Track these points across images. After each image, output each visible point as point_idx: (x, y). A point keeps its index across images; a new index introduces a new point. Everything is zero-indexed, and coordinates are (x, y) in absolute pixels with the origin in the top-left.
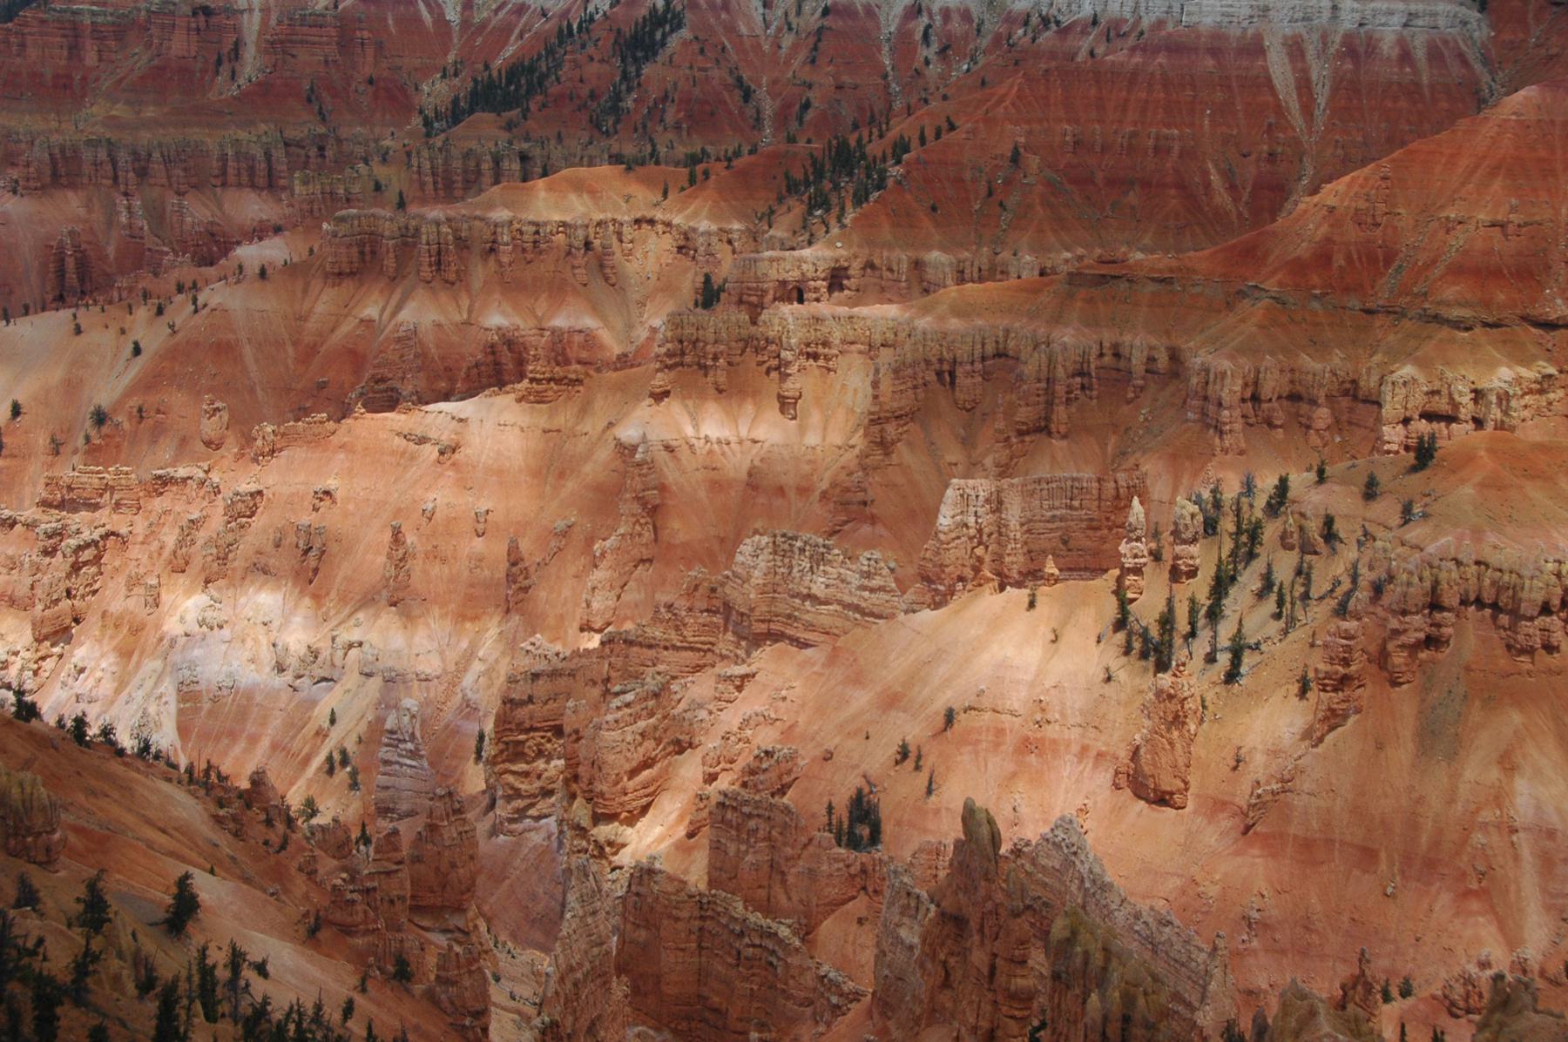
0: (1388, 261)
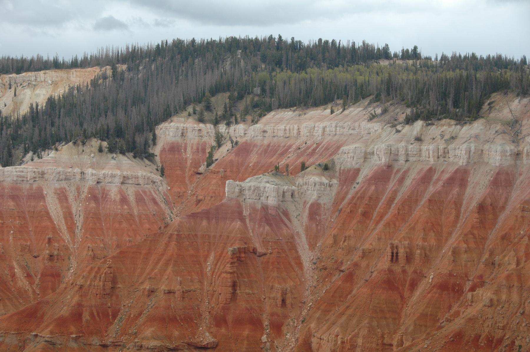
0: (114, 316)
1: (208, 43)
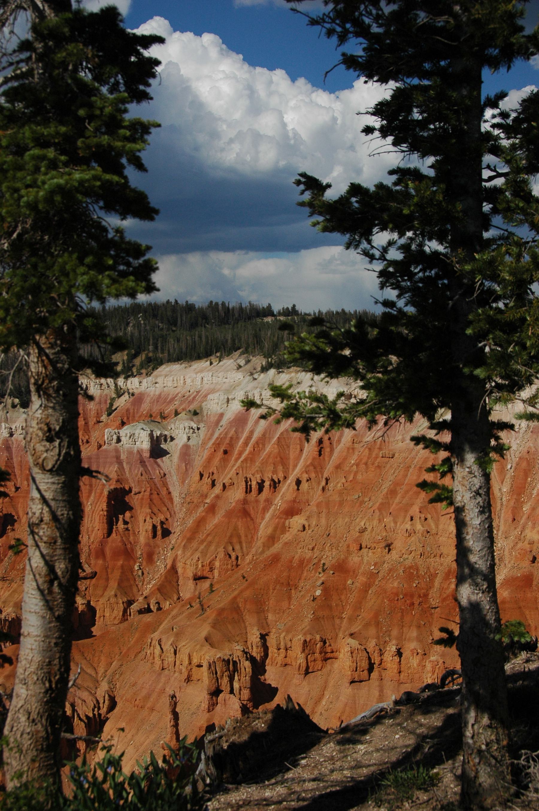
1: (115, 308)
